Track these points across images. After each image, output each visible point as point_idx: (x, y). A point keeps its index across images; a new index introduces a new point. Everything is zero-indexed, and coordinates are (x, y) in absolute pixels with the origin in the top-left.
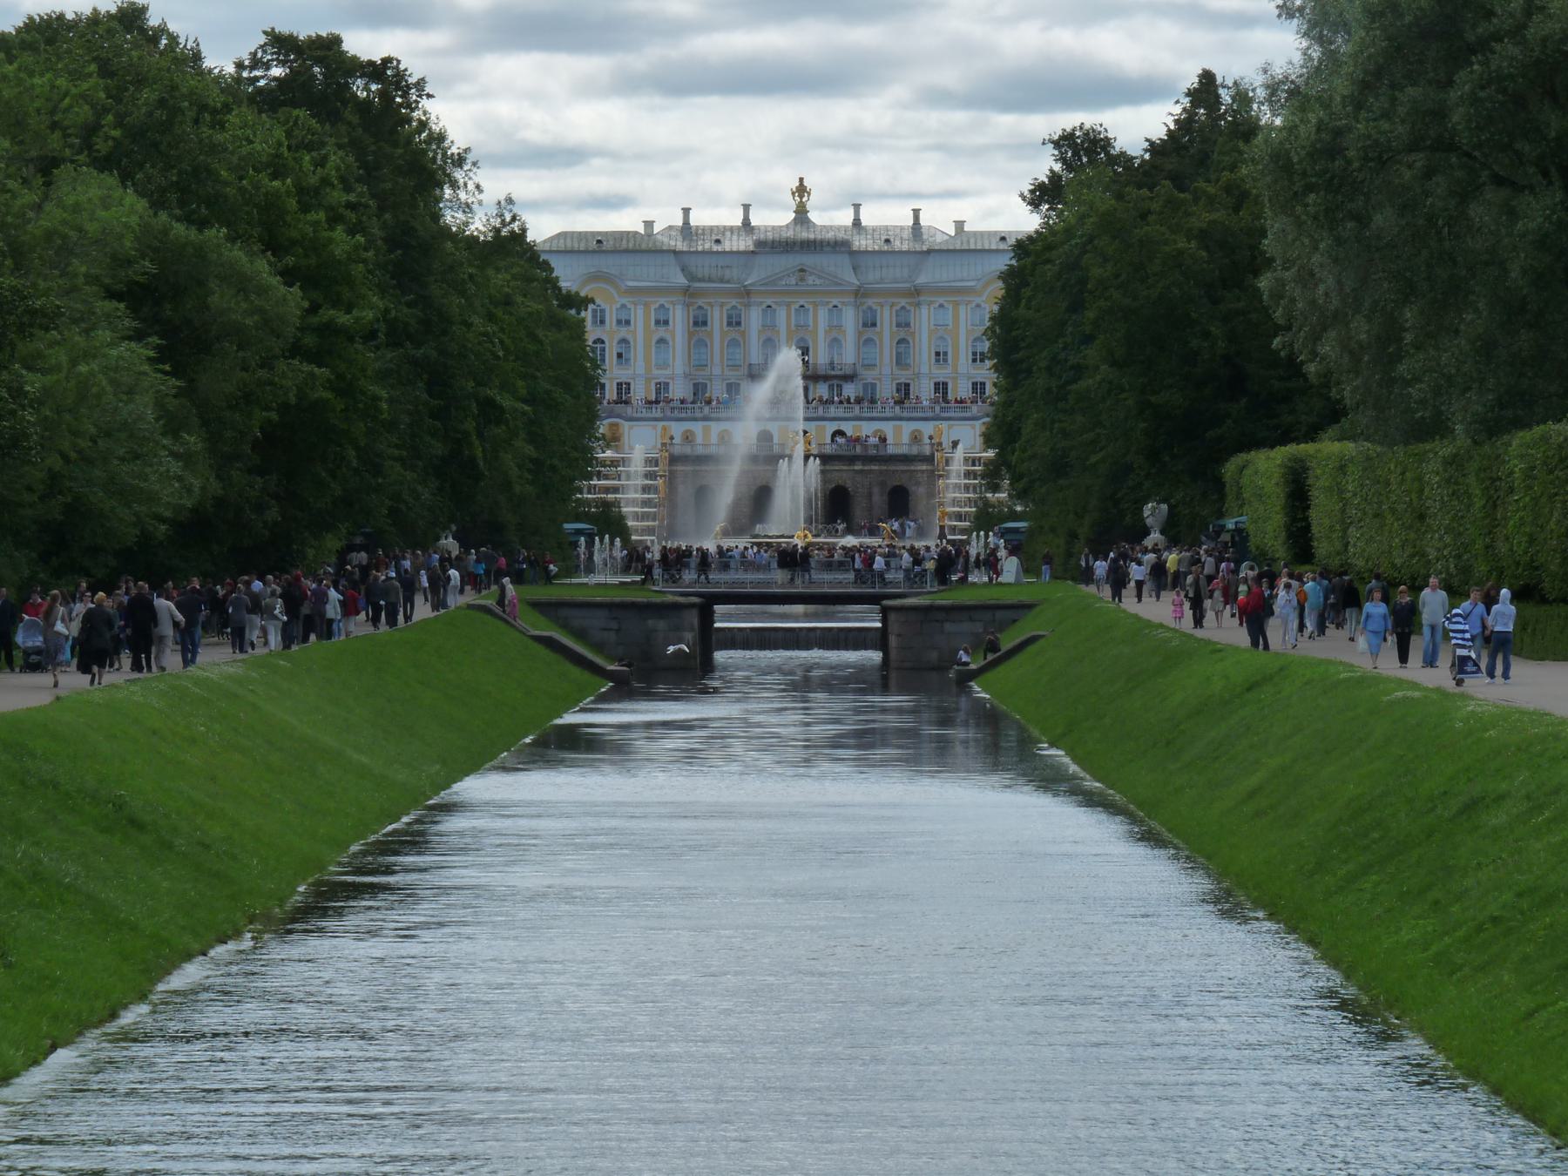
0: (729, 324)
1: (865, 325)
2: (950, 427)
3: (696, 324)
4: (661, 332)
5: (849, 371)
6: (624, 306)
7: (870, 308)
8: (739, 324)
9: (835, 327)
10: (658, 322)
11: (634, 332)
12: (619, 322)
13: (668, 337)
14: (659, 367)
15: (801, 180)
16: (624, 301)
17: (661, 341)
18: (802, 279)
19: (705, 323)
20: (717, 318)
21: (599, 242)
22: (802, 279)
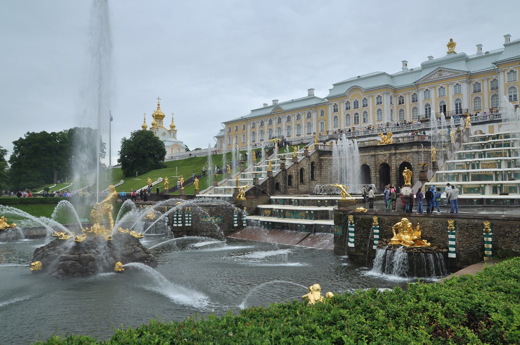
0: (413, 101)
1: (475, 92)
2: (500, 126)
3: (400, 103)
4: (379, 107)
5: (463, 113)
6: (365, 99)
7: (477, 83)
8: (417, 101)
9: (458, 93)
10: (378, 103)
11: (369, 108)
12: (364, 106)
13: (381, 108)
14: (378, 121)
15: (451, 40)
16: (365, 97)
17: (379, 110)
18: (440, 75)
19: (403, 103)
20: (408, 100)
21: (359, 77)
22: (440, 75)
